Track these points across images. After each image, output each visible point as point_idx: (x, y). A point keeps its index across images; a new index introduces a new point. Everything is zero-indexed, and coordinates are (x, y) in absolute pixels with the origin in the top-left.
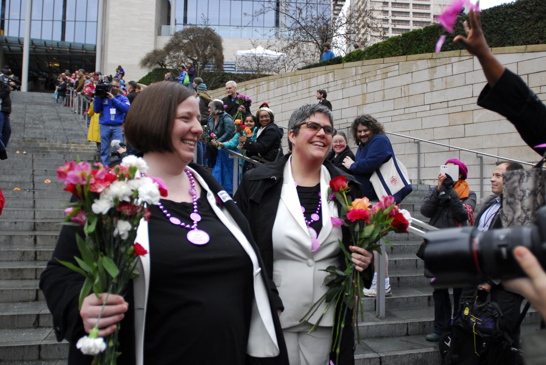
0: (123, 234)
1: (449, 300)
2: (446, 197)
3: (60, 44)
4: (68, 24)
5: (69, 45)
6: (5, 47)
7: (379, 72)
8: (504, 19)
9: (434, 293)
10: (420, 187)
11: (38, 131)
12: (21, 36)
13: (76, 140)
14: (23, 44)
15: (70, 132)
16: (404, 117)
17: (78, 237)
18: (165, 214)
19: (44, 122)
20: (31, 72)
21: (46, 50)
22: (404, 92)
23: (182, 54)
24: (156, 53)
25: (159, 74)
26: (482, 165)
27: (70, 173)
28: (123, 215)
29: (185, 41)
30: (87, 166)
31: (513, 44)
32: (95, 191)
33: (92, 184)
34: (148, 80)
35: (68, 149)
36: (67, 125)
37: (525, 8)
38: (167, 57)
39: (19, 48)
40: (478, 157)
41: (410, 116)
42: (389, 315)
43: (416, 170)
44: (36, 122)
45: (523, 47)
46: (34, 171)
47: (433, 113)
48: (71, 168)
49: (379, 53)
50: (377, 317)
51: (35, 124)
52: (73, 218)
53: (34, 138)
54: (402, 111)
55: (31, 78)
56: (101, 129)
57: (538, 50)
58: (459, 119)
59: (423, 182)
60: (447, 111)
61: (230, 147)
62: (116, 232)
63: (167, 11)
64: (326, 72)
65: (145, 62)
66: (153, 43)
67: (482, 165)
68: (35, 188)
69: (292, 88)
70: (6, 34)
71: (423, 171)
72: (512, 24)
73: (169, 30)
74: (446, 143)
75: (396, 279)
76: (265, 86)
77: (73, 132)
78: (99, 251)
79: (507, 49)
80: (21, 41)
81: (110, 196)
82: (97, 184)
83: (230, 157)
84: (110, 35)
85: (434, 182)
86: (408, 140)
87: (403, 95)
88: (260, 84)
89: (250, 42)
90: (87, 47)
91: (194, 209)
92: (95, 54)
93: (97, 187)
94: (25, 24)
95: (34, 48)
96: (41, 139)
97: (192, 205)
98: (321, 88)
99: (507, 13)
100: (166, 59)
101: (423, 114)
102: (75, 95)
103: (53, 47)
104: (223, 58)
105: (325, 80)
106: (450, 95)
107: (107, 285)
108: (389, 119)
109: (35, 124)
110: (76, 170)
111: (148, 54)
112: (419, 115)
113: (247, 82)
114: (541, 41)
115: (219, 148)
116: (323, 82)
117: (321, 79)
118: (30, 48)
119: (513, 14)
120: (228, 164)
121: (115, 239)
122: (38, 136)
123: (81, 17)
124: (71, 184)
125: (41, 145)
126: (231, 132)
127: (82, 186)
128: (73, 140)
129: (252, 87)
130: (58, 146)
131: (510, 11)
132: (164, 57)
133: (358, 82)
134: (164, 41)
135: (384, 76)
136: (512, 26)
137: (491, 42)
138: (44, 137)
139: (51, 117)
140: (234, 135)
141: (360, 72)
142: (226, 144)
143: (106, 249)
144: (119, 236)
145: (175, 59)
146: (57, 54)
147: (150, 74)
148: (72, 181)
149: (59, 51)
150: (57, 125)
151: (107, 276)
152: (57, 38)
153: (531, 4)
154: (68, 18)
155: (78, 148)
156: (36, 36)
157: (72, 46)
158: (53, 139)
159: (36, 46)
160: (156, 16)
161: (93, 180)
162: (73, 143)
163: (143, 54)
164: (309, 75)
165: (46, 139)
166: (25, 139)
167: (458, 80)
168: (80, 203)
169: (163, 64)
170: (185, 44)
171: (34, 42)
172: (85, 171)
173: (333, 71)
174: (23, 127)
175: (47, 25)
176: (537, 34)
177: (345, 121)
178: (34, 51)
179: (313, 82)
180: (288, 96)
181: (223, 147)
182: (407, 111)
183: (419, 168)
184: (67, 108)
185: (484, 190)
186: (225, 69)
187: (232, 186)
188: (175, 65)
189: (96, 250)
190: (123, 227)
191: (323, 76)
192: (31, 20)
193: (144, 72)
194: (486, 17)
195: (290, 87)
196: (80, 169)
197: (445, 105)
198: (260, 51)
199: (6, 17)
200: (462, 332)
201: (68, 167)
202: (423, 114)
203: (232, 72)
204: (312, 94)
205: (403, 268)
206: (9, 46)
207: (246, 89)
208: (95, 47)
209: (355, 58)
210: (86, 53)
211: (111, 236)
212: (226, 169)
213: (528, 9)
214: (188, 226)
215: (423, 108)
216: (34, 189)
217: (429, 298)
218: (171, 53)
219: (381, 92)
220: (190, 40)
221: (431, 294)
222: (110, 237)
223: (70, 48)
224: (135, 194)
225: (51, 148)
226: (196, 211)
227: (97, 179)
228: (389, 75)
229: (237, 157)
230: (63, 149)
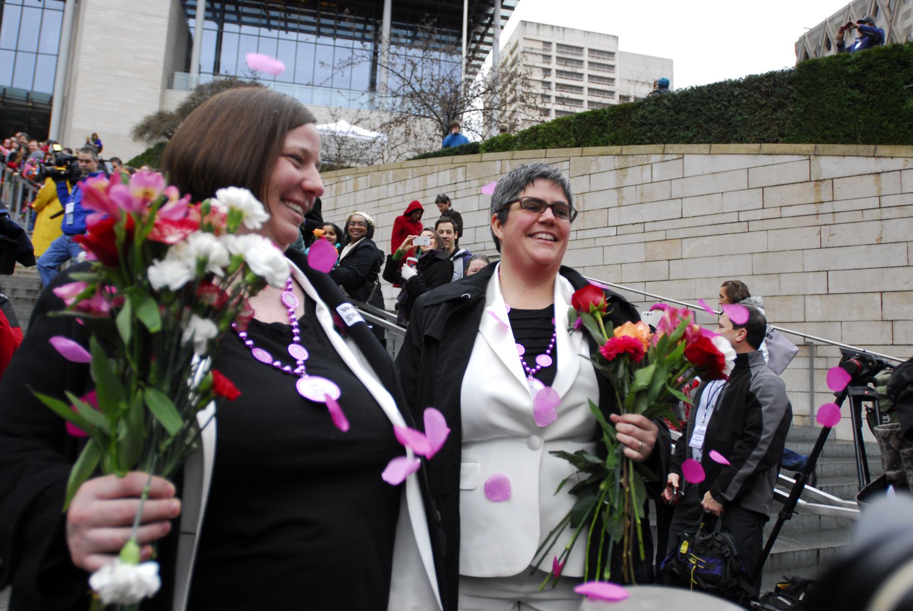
8: (729, 102)
31: (741, 140)
37: (758, 88)
41: (586, 244)
45: (756, 146)
47: (621, 239)
49: (539, 140)
57: (777, 152)
58: (660, 250)
60: (641, 237)
63: (185, 49)
64: (453, 166)
65: (141, 132)
66: (157, 99)
69: (396, 188)
72: (740, 111)
73: (188, 82)
76: (350, 185)
79: (733, 147)
88: (343, 179)
92: (50, 111)
99: (733, 94)
105: (451, 179)
111: (148, 118)
112: (599, 242)
114: (781, 140)
116: (448, 182)
117: (443, 177)
134: (177, 99)
136: (740, 114)
137: (709, 135)
147: (148, 152)
153: (767, 84)
157: (8, 92)
160: (166, 54)
163: (138, 118)
164: (425, 170)
167: (661, 191)
173: (464, 165)
176: (776, 128)
179: (432, 181)
191: (448, 172)
193: (140, 148)
195: (392, 187)
197: (640, 228)
208: (51, 98)
213: (763, 90)
215: (605, 232)
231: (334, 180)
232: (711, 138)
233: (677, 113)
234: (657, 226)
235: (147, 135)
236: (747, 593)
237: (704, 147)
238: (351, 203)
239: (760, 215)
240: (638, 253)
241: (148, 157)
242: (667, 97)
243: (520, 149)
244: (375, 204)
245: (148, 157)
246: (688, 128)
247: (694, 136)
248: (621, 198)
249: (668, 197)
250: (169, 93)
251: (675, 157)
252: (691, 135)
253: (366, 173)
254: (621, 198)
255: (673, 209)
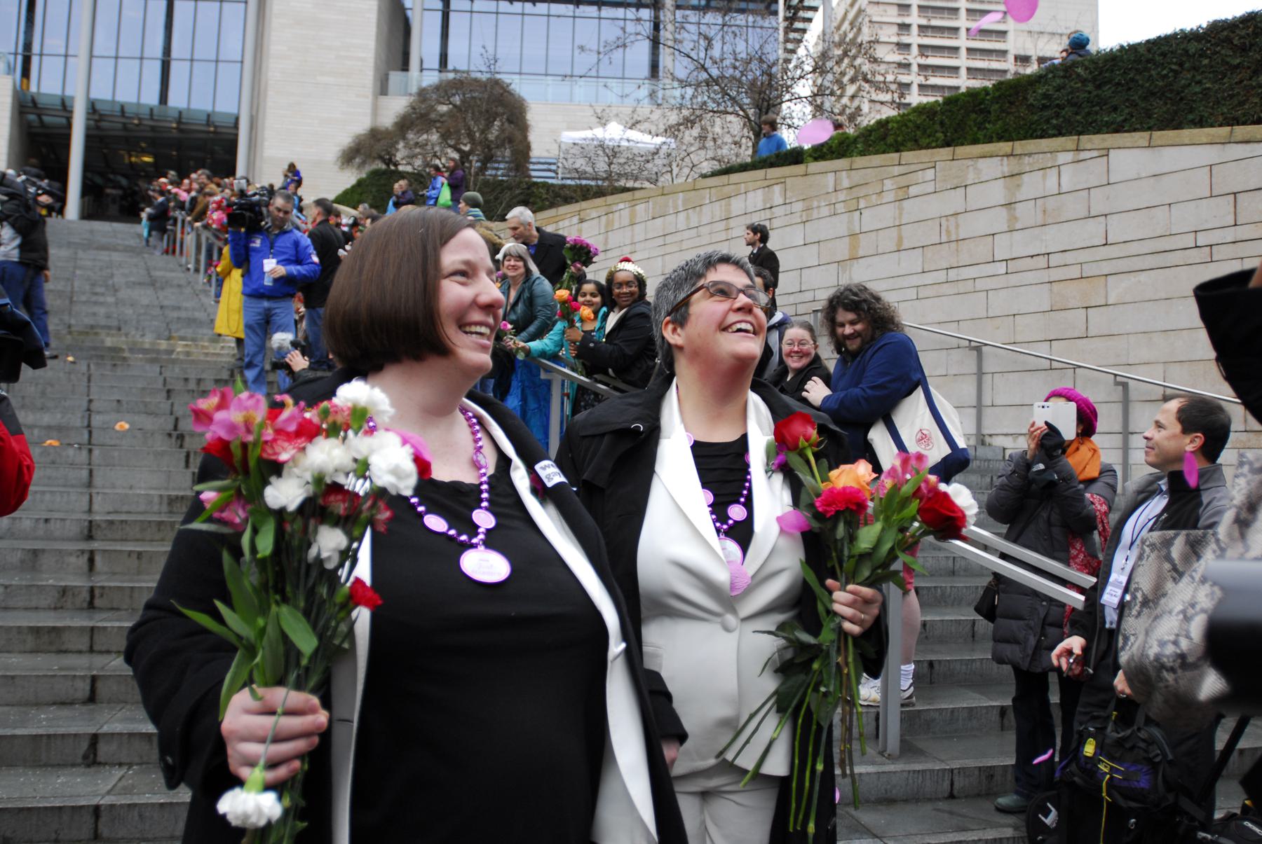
0: (329, 558)
1: (1051, 717)
2: (1047, 476)
3: (155, 112)
4: (174, 66)
5: (176, 115)
6: (32, 117)
7: (888, 184)
8: (1181, 65)
9: (1014, 700)
10: (982, 452)
11: (102, 311)
12: (68, 93)
13: (188, 332)
14: (71, 112)
15: (175, 314)
16: (946, 289)
17: (226, 557)
18: (413, 507)
19: (116, 291)
20: (89, 175)
21: (124, 124)
22: (948, 232)
23: (435, 137)
24: (375, 134)
25: (382, 182)
26: (1126, 402)
27: (219, 416)
28: (332, 513)
29: (444, 108)
30: (258, 401)
31: (1200, 123)
32: (273, 457)
33: (266, 442)
34: (356, 197)
35: (171, 352)
36: (169, 297)
37: (1228, 40)
38: (401, 145)
39: (64, 121)
40: (1117, 384)
41: (962, 287)
42: (908, 749)
43: (974, 411)
44: (99, 290)
46: (90, 401)
47: (1014, 279)
48: (223, 405)
49: (890, 140)
50: (881, 753)
51: (96, 294)
52: (216, 515)
53: (92, 327)
54: (941, 276)
55: (88, 189)
56: (246, 307)
58: (1073, 294)
59: (988, 440)
60: (1045, 276)
61: (543, 354)
62: (313, 552)
63: (401, 40)
64: (767, 183)
65: (350, 156)
66: (368, 110)
67: (1126, 402)
68: (93, 441)
69: (688, 218)
70: (33, 89)
71: (987, 413)
72: (1198, 78)
74: (1043, 350)
75: (926, 665)
77: (183, 314)
78: (271, 591)
80: (68, 103)
81: (306, 470)
82: (279, 442)
83: (543, 376)
84: (270, 93)
85: (1015, 441)
86: (955, 342)
87: (944, 239)
88: (615, 208)
89: (590, 112)
90: (214, 119)
91: (482, 500)
92: (237, 135)
93: (278, 449)
94: (78, 65)
95: (96, 121)
96: (109, 328)
97: (475, 490)
98: (756, 219)
100: (397, 150)
101: (990, 283)
102: (188, 229)
103: (140, 119)
104: (528, 147)
105: (764, 201)
106: (1053, 239)
107: (286, 668)
108: (912, 294)
109: (96, 294)
110: (232, 408)
111: (358, 137)
112: (980, 284)
113: (584, 204)
115: (521, 356)
117: (754, 198)
118: (88, 119)
119: (1203, 54)
120: (540, 392)
121: (309, 566)
122: (103, 322)
123: (205, 50)
124: (220, 439)
125: (109, 342)
126: (550, 318)
127: (244, 446)
128: (182, 333)
129: (594, 214)
130: (147, 346)
131: (1193, 47)
132: (393, 145)
133: (840, 208)
134: (395, 107)
135: (901, 194)
136: (1199, 82)
137: (1149, 117)
138: (115, 323)
139: (132, 279)
140: (554, 324)
141: (846, 183)
142: (535, 345)
143: (288, 589)
144: (319, 561)
145: (418, 150)
146: (150, 134)
147: (360, 183)
148: (223, 434)
149: (153, 129)
150: (145, 296)
151: (289, 650)
152: (151, 97)
153: (1243, 33)
154: (175, 53)
155: (193, 350)
156: (102, 92)
157: (184, 115)
158: (137, 329)
159: (101, 115)
161: (269, 434)
162: (182, 339)
163: (344, 139)
164: (727, 190)
165: (119, 329)
166: (73, 329)
167: (1073, 206)
168: (235, 480)
169: (390, 160)
170: (442, 115)
171: (98, 107)
172: (252, 412)
173: (782, 181)
174: (67, 302)
175: (128, 69)
176: (1256, 100)
177: (808, 296)
178: (98, 128)
179: (737, 205)
180: (677, 237)
181: (528, 352)
182: (953, 274)
183: (979, 407)
184: (170, 257)
185: (1131, 462)
186: (533, 174)
187: (547, 444)
188: (418, 162)
189: (265, 586)
190: (329, 541)
191: (760, 192)
192: (91, 56)
193: (348, 179)
194: (1138, 60)
195: (682, 216)
196: (241, 407)
197: (1042, 262)
198: (614, 132)
199: (36, 48)
200: (1077, 791)
201: (215, 400)
202: (990, 283)
203: (550, 181)
204: (735, 233)
205: (942, 640)
206: (39, 116)
207: (582, 221)
208: (237, 119)
209: (833, 152)
210: (214, 132)
211: (302, 559)
212: (532, 405)
214: (464, 538)
216: (90, 443)
217: (1003, 711)
218: (410, 135)
219: (894, 232)
220: (455, 106)
221: (1008, 702)
222: (300, 562)
223: (179, 121)
224: (362, 468)
225: (131, 350)
226: (485, 504)
227: (279, 432)
228: (913, 191)
229: (560, 378)
230: (158, 352)
231: (603, 211)
232: (1152, 122)
233: (1099, 87)
234: (1069, 258)
235: (357, 160)
236: (1193, 819)
237: (1141, 137)
238: (628, 242)
239: (1229, 235)
240: (1039, 299)
241: (359, 190)
242: (1083, 65)
243: (863, 153)
244: (660, 241)
245: (359, 190)
246: (1115, 109)
247: (1125, 120)
248: (1013, 218)
249: (1084, 213)
250: (383, 99)
251: (1095, 154)
252: (1120, 119)
253: (647, 199)
254: (1013, 218)
255: (1092, 232)
